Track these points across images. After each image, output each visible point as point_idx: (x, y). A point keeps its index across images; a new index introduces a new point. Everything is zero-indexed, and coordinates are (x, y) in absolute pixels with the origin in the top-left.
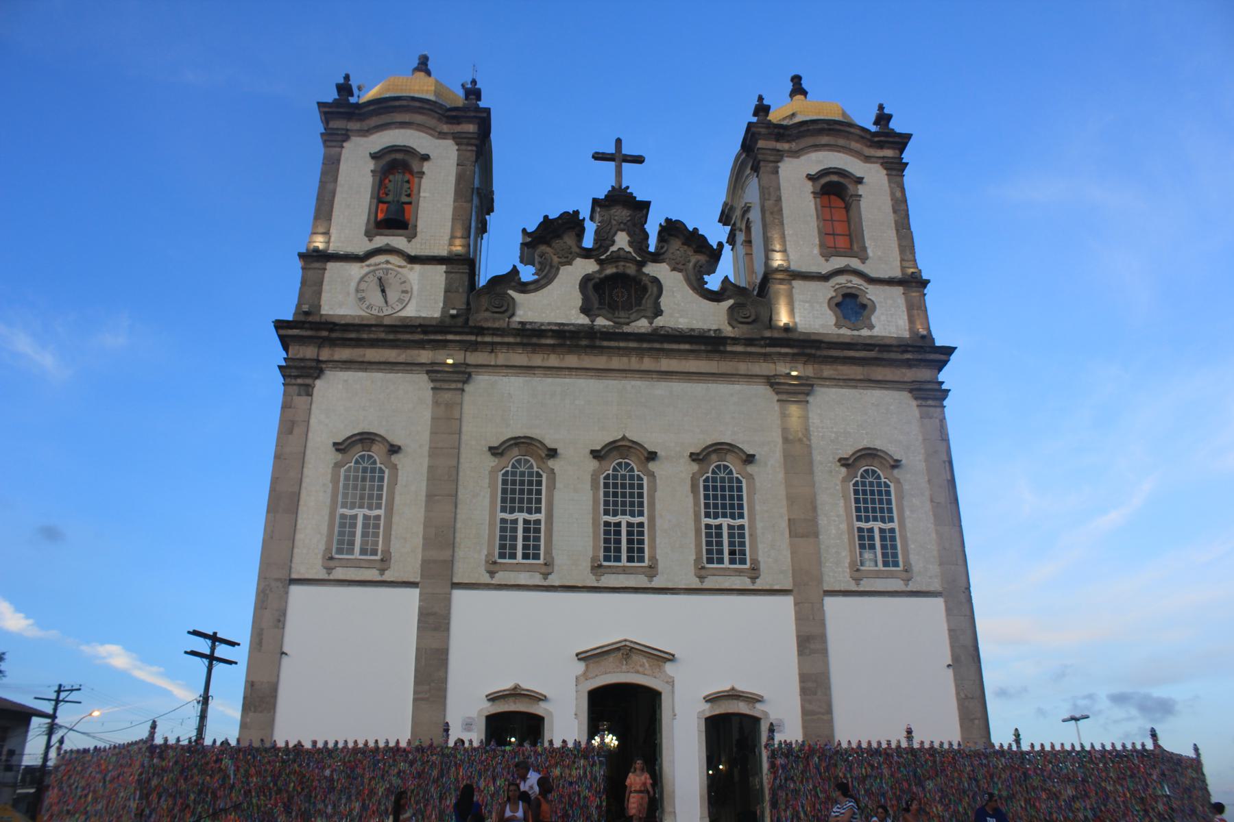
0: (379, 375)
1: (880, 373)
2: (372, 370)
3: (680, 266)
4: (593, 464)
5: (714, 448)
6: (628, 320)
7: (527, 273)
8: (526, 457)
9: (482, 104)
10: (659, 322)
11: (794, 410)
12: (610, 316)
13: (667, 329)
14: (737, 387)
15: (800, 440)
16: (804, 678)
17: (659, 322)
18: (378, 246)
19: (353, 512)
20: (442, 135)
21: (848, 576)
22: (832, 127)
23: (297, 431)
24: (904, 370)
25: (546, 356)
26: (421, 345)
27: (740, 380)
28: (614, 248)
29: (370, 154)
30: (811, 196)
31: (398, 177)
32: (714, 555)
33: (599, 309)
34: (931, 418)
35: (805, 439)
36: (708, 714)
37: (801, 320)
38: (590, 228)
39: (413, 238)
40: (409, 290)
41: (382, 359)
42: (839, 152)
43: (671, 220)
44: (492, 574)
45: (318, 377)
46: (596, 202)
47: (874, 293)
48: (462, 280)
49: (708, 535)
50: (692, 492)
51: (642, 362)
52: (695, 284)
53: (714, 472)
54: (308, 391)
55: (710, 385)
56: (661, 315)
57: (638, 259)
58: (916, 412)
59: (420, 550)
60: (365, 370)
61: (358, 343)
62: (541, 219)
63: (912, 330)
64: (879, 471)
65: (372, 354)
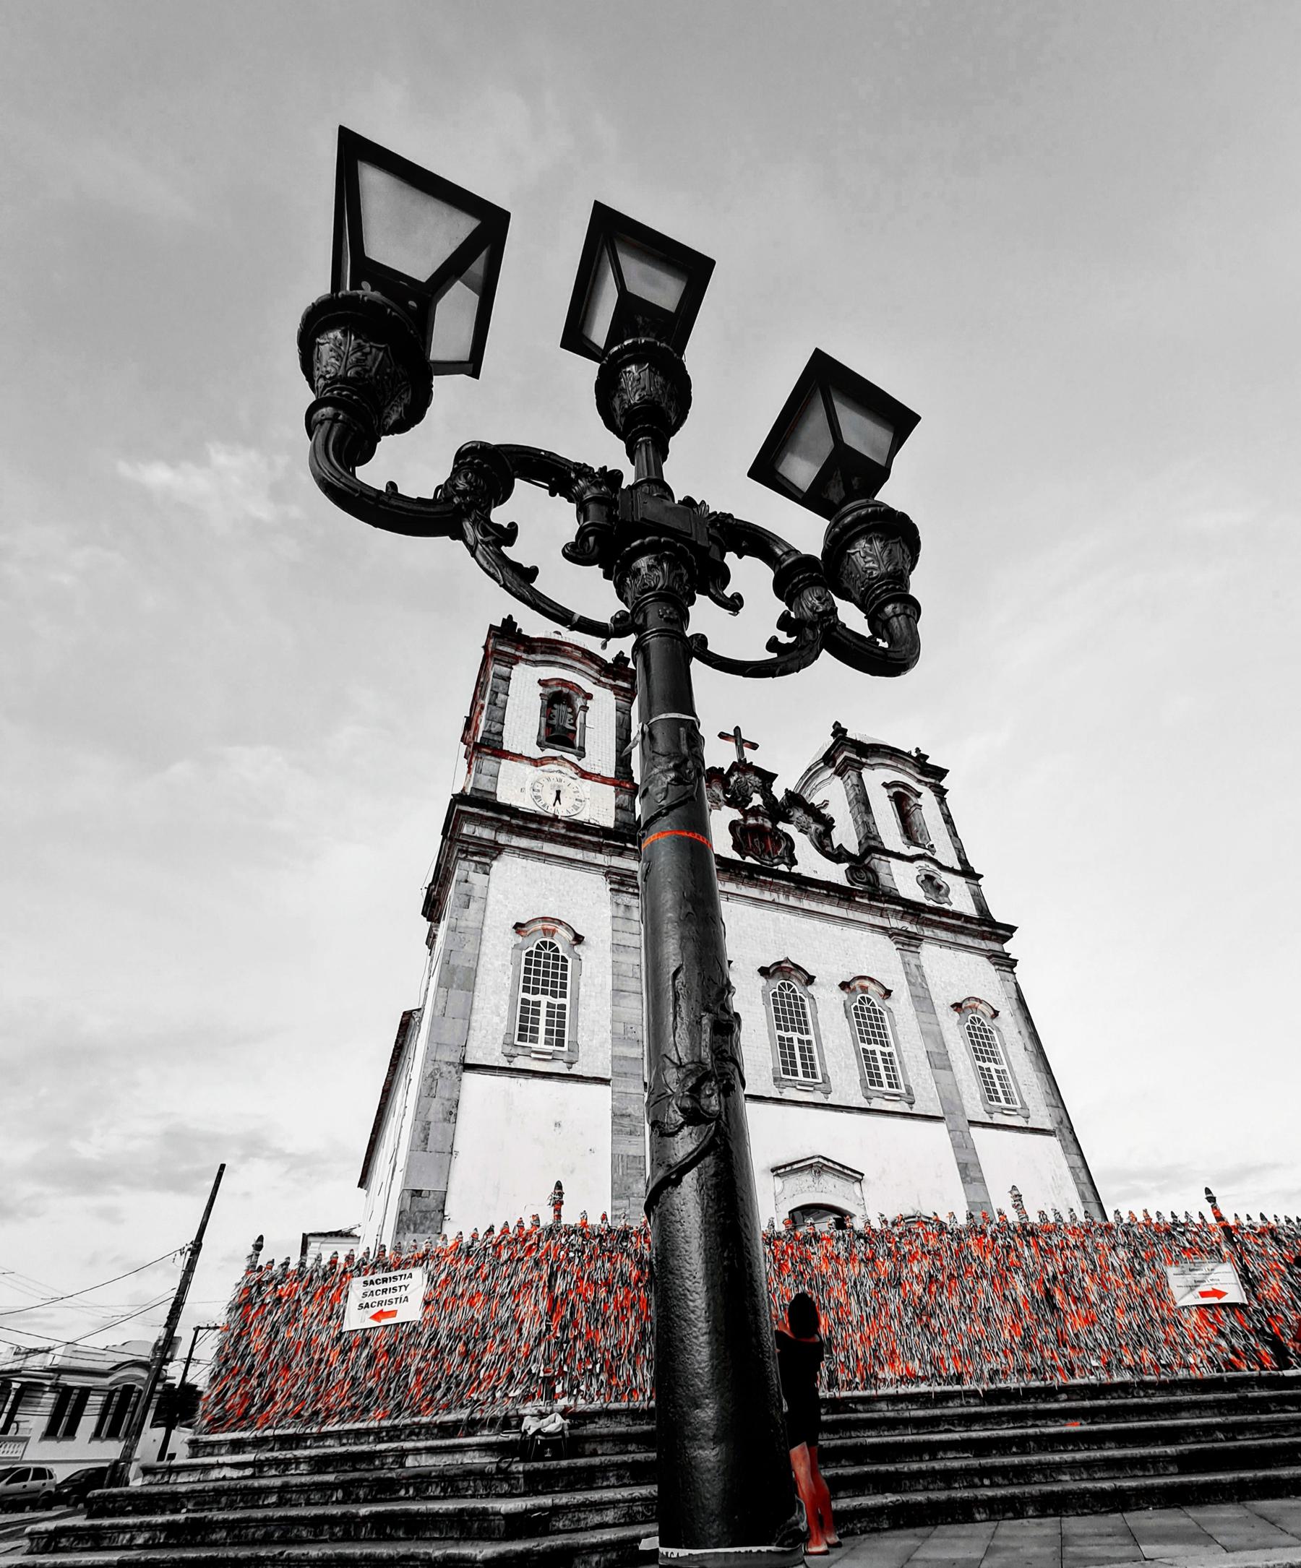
1: (963, 940)
2: (551, 863)
10: (795, 869)
26: (598, 848)
45: (494, 859)
47: (945, 878)
61: (536, 835)
65: (549, 848)
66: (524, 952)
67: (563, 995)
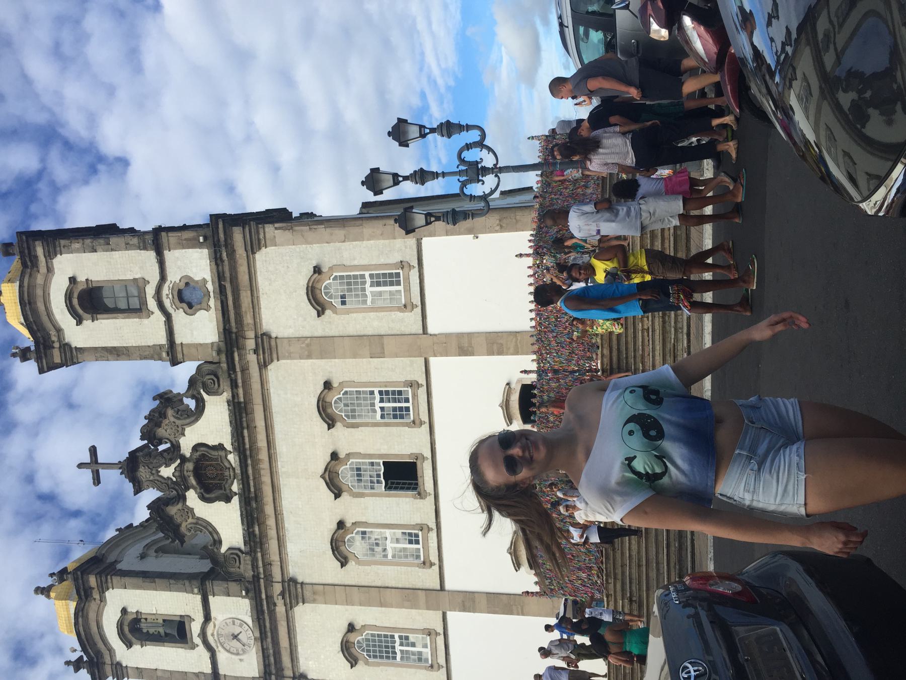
1: (243, 277)
3: (180, 429)
5: (322, 413)
6: (231, 470)
10: (228, 446)
11: (283, 348)
12: (229, 481)
13: (233, 441)
14: (272, 390)
16: (490, 353)
17: (228, 446)
21: (409, 314)
22: (27, 302)
24: (238, 256)
25: (268, 528)
26: (272, 613)
27: (266, 388)
28: (174, 479)
30: (96, 321)
31: (143, 626)
33: (225, 490)
34: (275, 237)
35: (306, 342)
39: (190, 617)
41: (287, 636)
42: (49, 294)
44: (432, 564)
47: (174, 276)
48: (218, 586)
52: (193, 419)
56: (223, 445)
57: (179, 461)
58: (271, 249)
59: (420, 611)
60: (296, 647)
65: (284, 642)
67: (392, 637)
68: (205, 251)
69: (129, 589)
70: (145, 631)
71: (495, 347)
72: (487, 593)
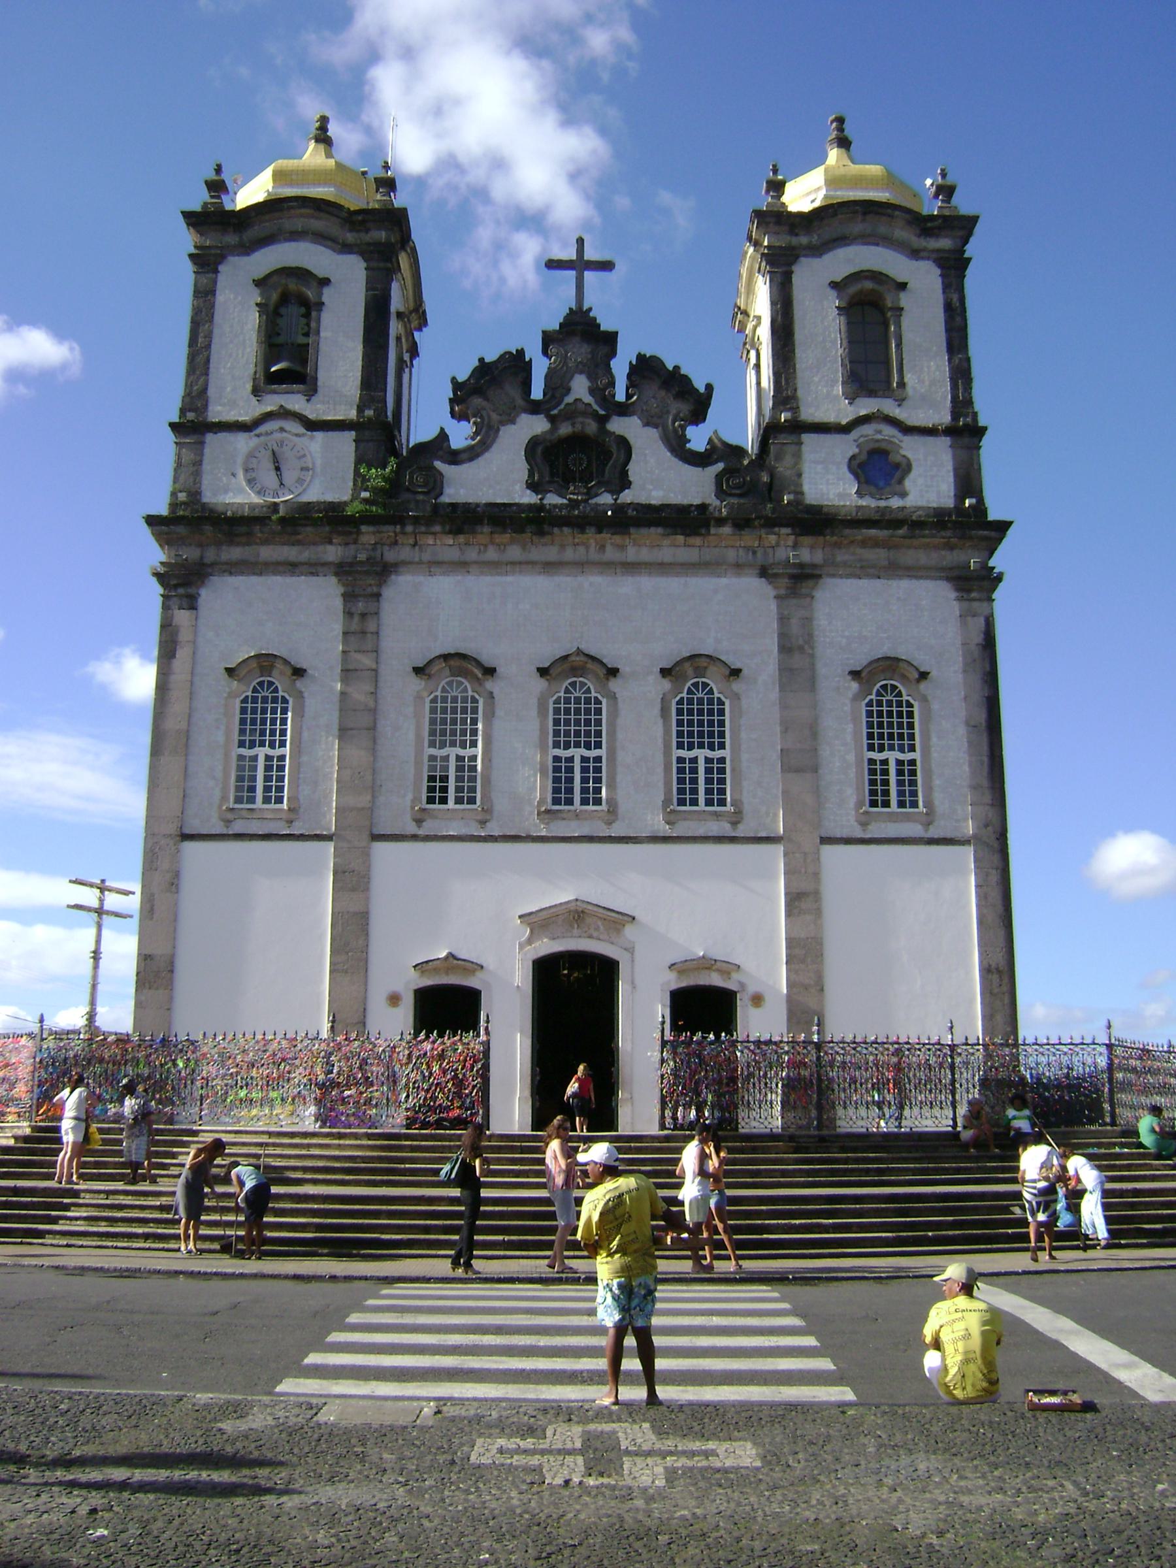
0: (278, 579)
1: (909, 557)
4: (541, 684)
7: (461, 435)
8: (459, 679)
9: (398, 202)
10: (627, 497)
14: (724, 581)
15: (801, 649)
17: (627, 497)
18: (269, 409)
19: (252, 752)
20: (345, 248)
23: (180, 653)
25: (482, 548)
28: (569, 399)
29: (254, 281)
32: (685, 794)
36: (674, 986)
37: (810, 489)
38: (540, 367)
40: (311, 466)
42: (877, 245)
43: (645, 355)
46: (546, 335)
47: (911, 448)
49: (681, 771)
50: (662, 716)
51: (604, 552)
53: (690, 692)
54: (191, 603)
55: (688, 579)
56: (629, 488)
58: (955, 608)
62: (477, 363)
63: (960, 497)
64: (901, 687)
65: (267, 553)
66: (238, 701)
68: (949, 502)
69: (366, 296)
70: (283, 311)
71: (797, 951)
72: (367, 913)
